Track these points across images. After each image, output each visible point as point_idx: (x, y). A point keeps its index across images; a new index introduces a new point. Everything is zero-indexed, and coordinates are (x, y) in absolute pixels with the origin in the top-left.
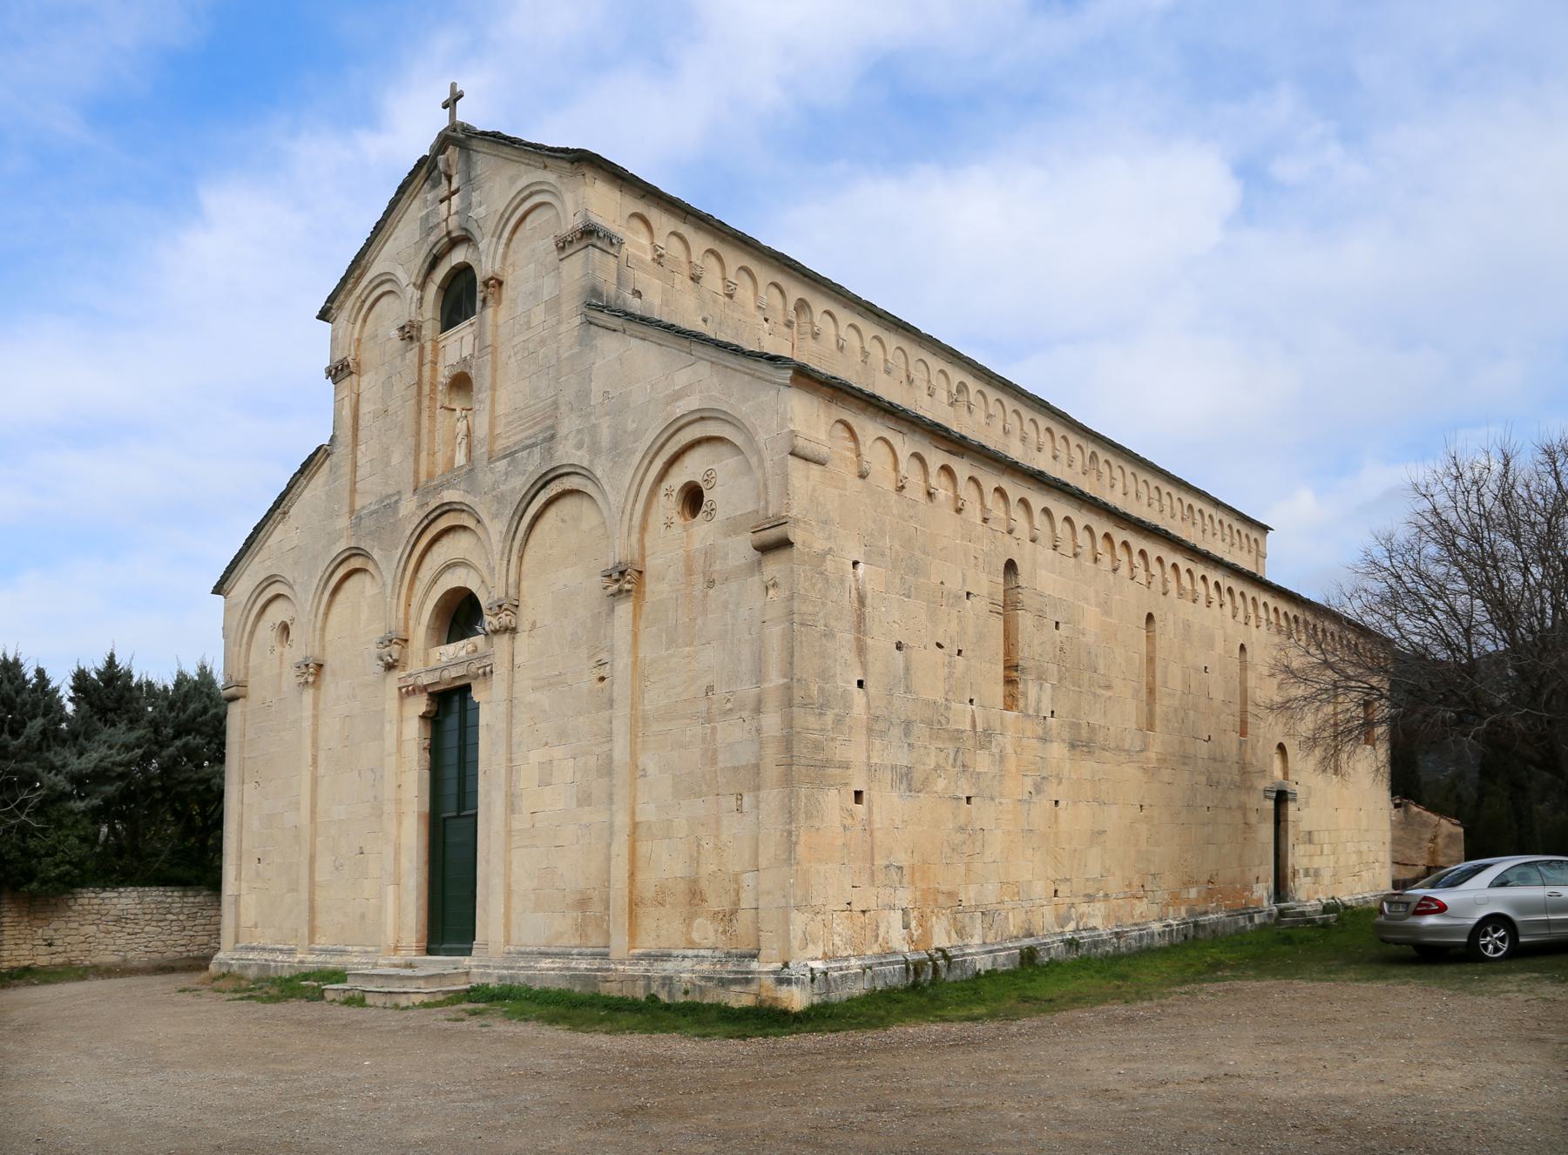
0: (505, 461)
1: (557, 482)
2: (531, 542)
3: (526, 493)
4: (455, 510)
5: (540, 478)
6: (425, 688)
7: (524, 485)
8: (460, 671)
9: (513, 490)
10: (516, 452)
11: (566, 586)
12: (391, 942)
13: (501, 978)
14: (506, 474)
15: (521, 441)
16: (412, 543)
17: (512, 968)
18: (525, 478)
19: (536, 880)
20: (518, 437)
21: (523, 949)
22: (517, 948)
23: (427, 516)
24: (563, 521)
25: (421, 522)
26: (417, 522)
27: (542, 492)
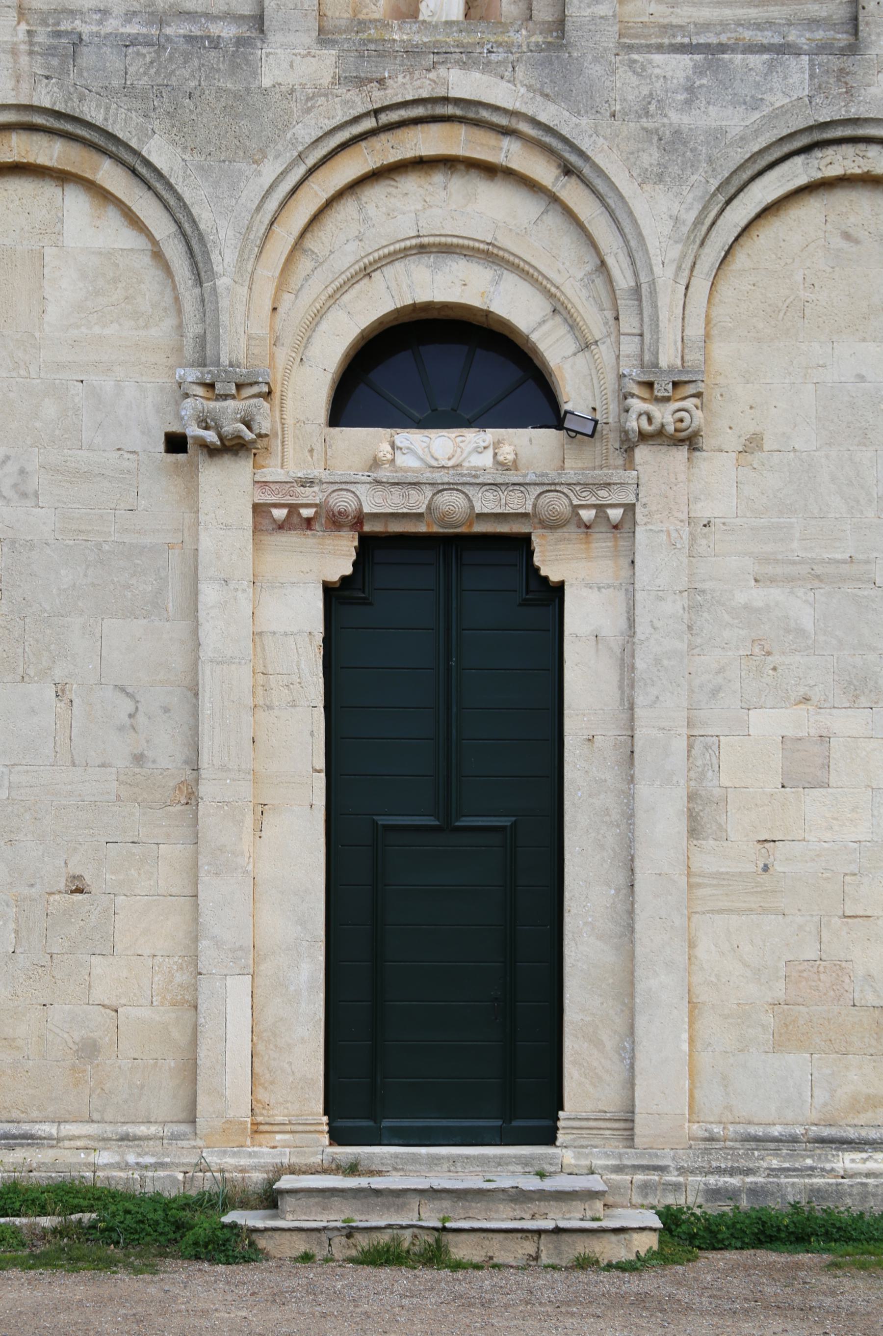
0: (685, 61)
1: (848, 150)
2: (741, 259)
3: (761, 152)
4: (478, 123)
5: (810, 129)
6: (360, 519)
7: (757, 133)
8: (516, 503)
9: (717, 135)
10: (722, 48)
11: (861, 378)
12: (241, 1111)
13: (714, 1194)
14: (690, 89)
15: (724, 25)
16: (311, 161)
17: (748, 1172)
18: (757, 115)
19: (781, 984)
20: (706, 14)
21: (752, 1130)
22: (741, 1129)
23: (376, 112)
24: (847, 236)
25: (356, 120)
26: (339, 119)
27: (799, 160)
